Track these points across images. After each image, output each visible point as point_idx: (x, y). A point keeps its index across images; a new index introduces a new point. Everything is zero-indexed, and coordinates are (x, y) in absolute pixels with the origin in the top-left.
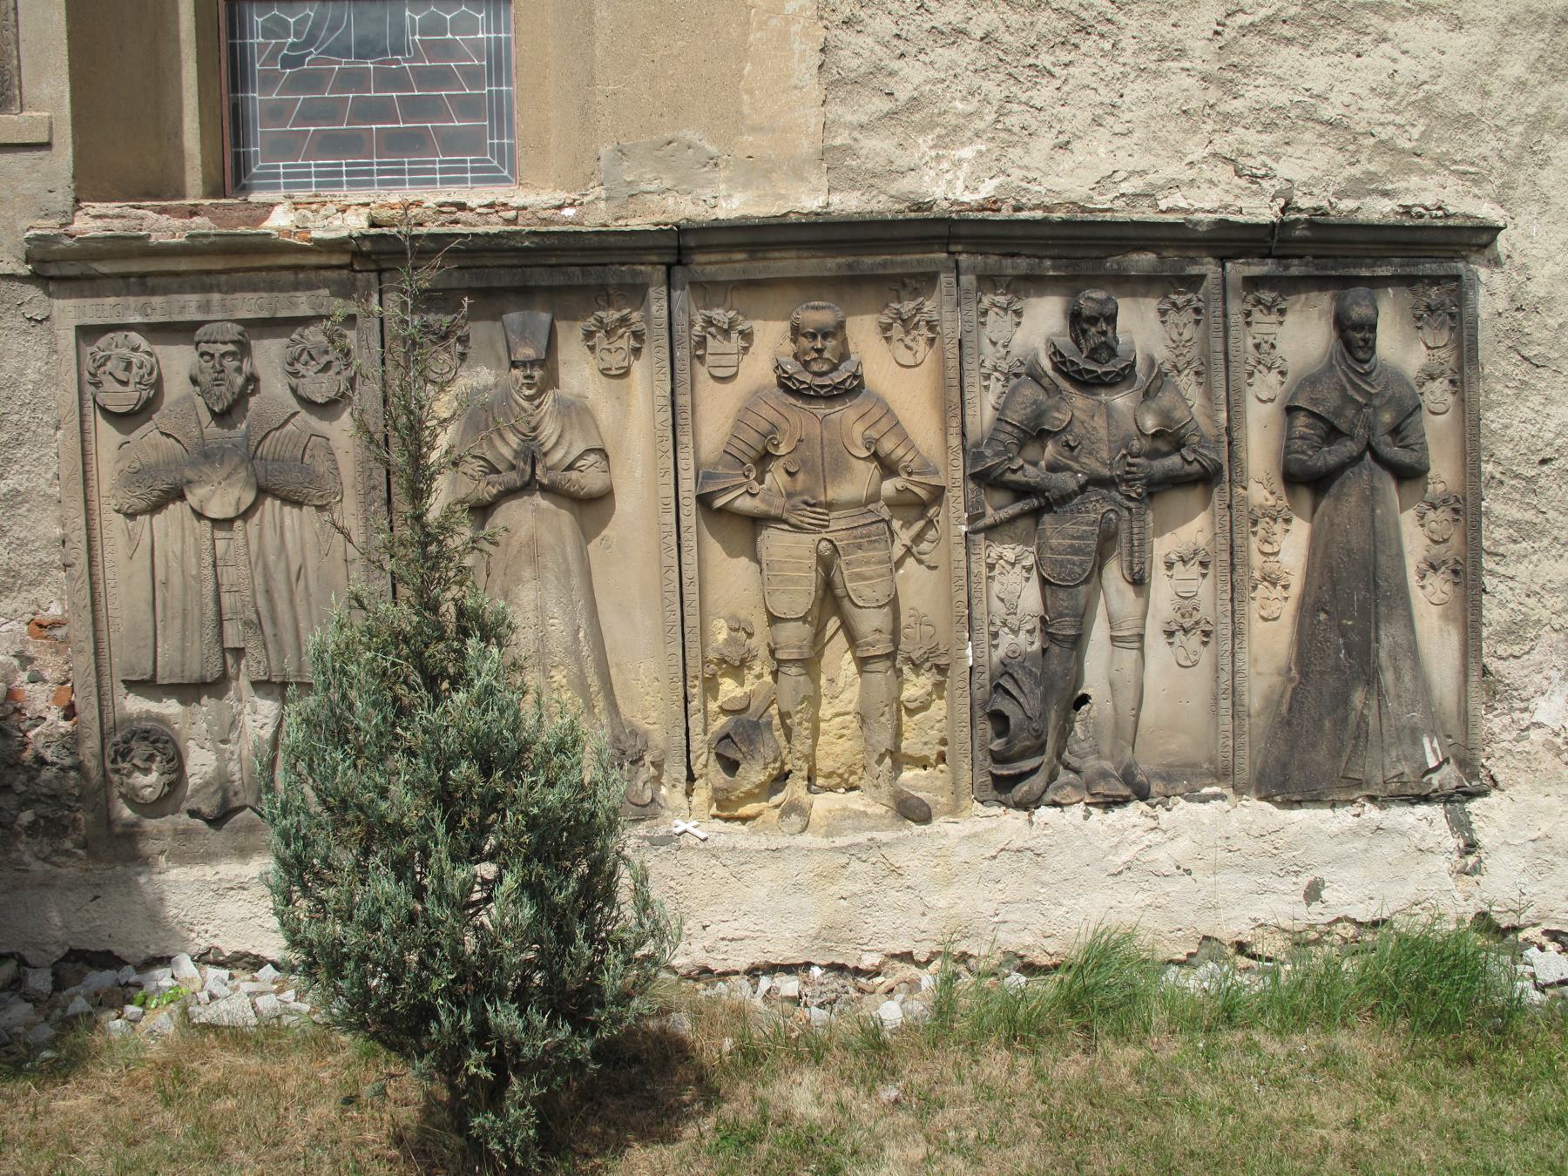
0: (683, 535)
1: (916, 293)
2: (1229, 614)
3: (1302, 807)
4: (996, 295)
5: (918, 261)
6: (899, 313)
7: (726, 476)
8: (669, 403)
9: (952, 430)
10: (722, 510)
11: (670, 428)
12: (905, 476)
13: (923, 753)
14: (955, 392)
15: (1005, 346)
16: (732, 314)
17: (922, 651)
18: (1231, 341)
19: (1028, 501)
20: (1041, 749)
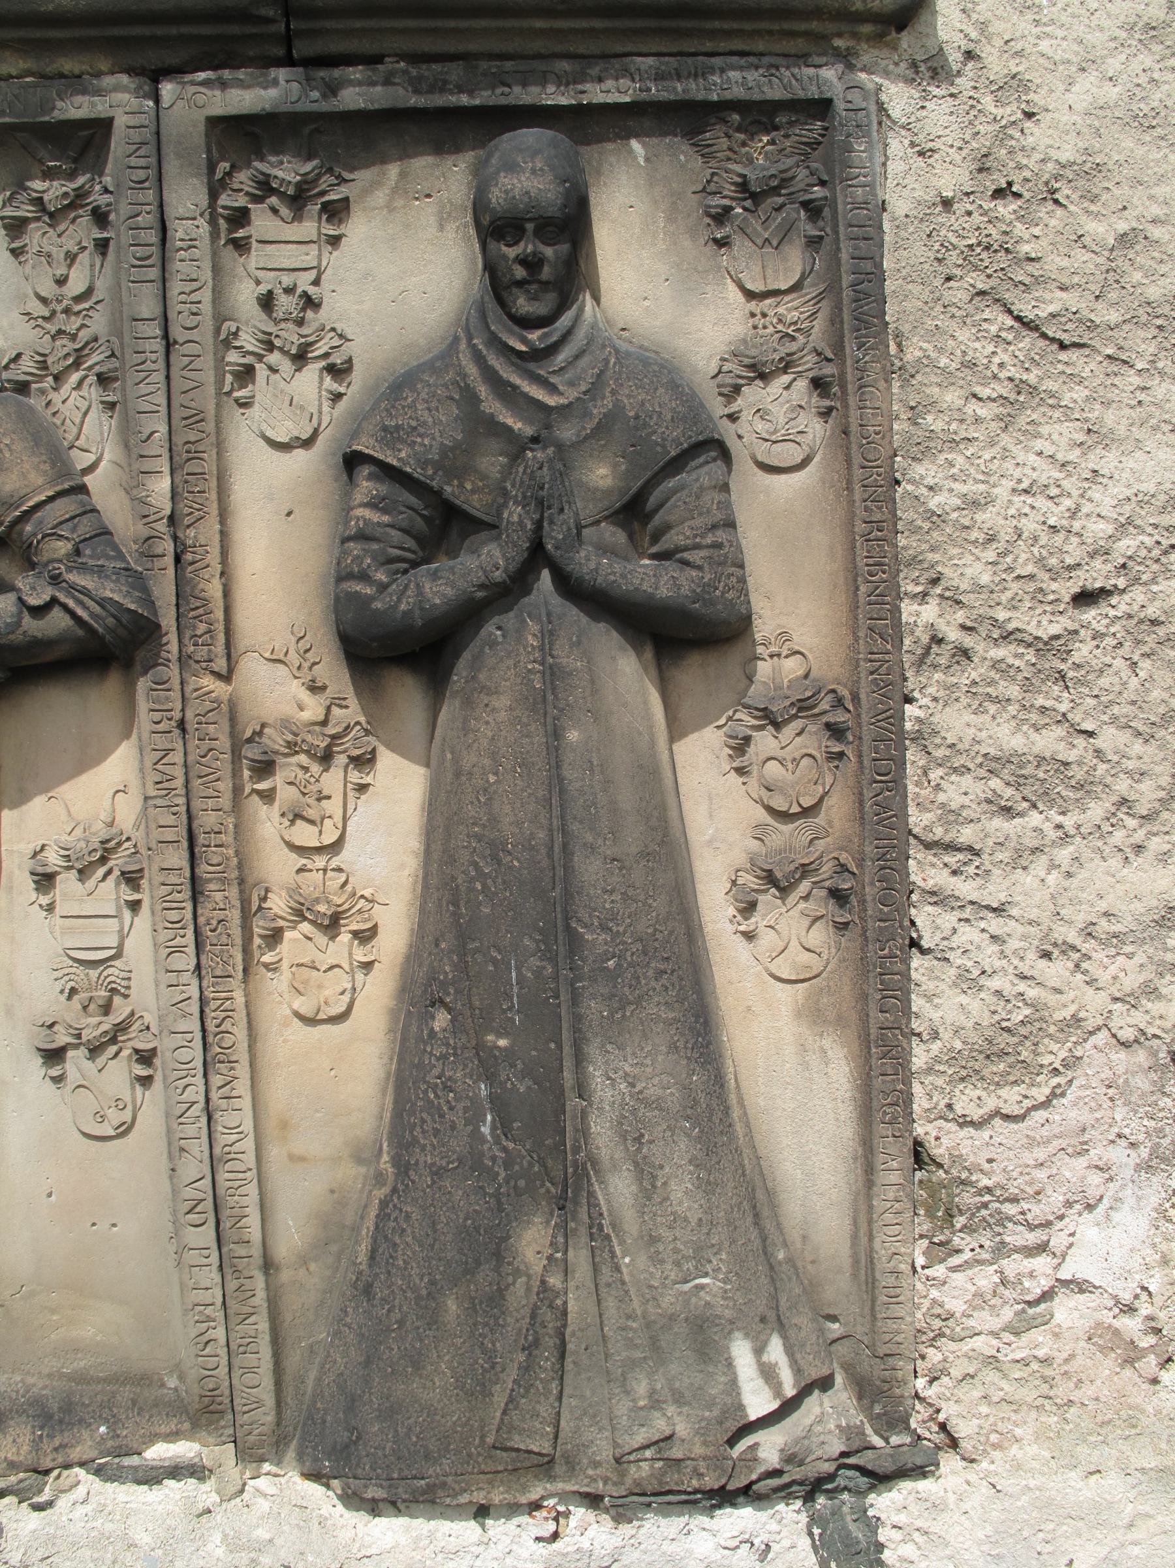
2: (195, 1008)
3: (399, 1512)
18: (176, 288)
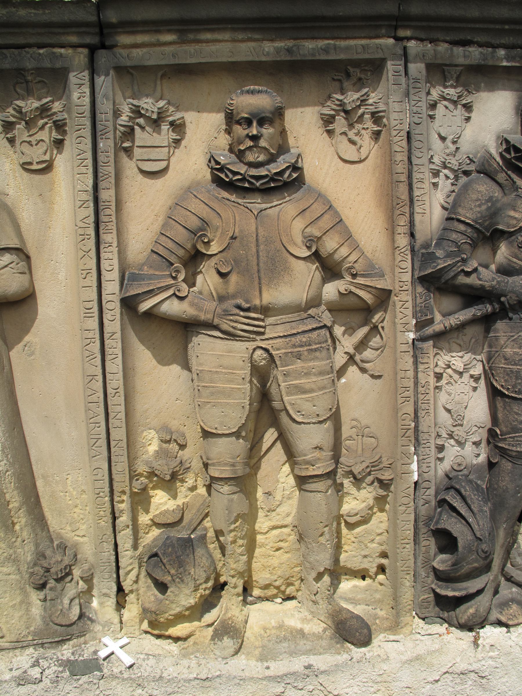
0: (107, 342)
1: (360, 83)
4: (446, 87)
5: (363, 46)
6: (342, 104)
7: (150, 277)
8: (91, 198)
9: (400, 230)
10: (149, 314)
11: (92, 226)
12: (349, 278)
13: (363, 566)
14: (403, 189)
15: (454, 142)
16: (161, 104)
17: (364, 465)
19: (480, 306)
20: (487, 568)
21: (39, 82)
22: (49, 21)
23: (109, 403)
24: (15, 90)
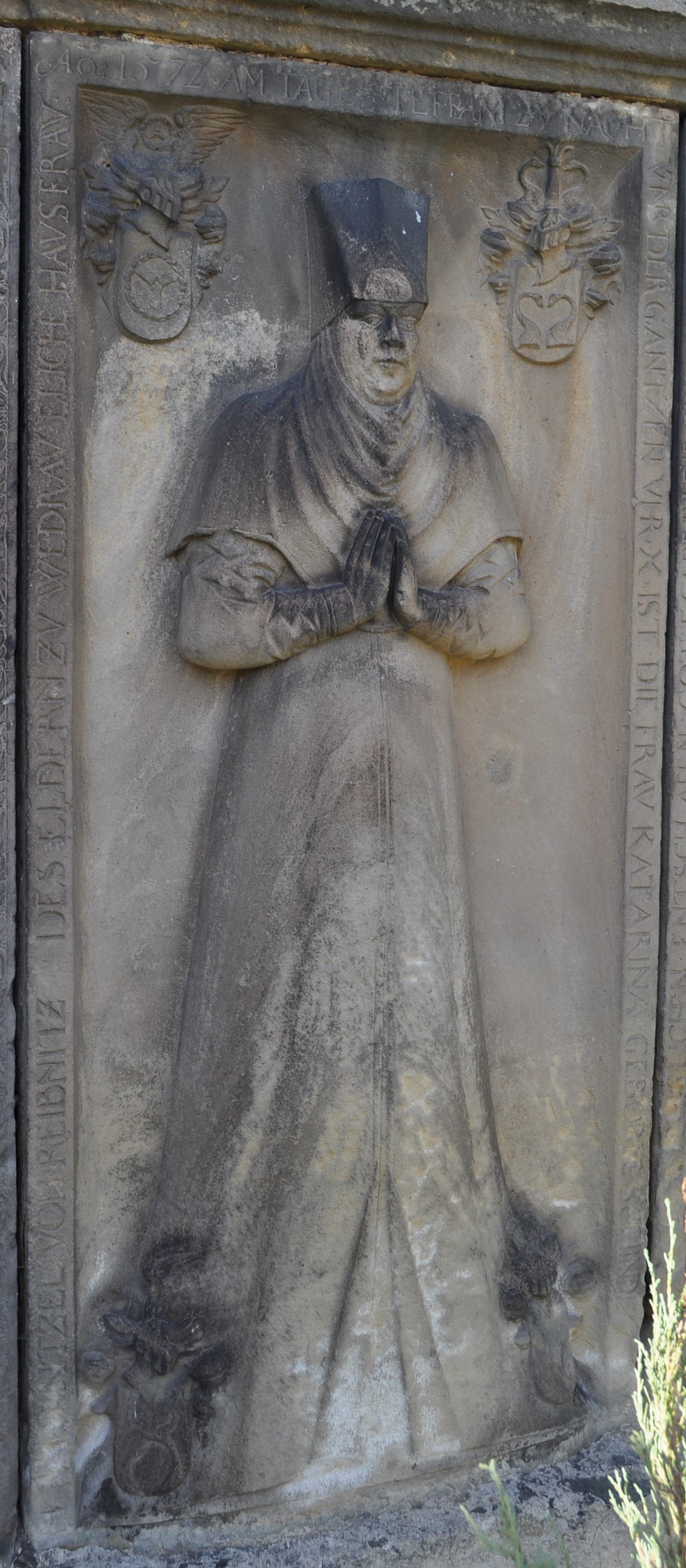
11: (665, 500)
21: (573, 169)
22: (639, 49)
23: (671, 889)
24: (520, 179)
